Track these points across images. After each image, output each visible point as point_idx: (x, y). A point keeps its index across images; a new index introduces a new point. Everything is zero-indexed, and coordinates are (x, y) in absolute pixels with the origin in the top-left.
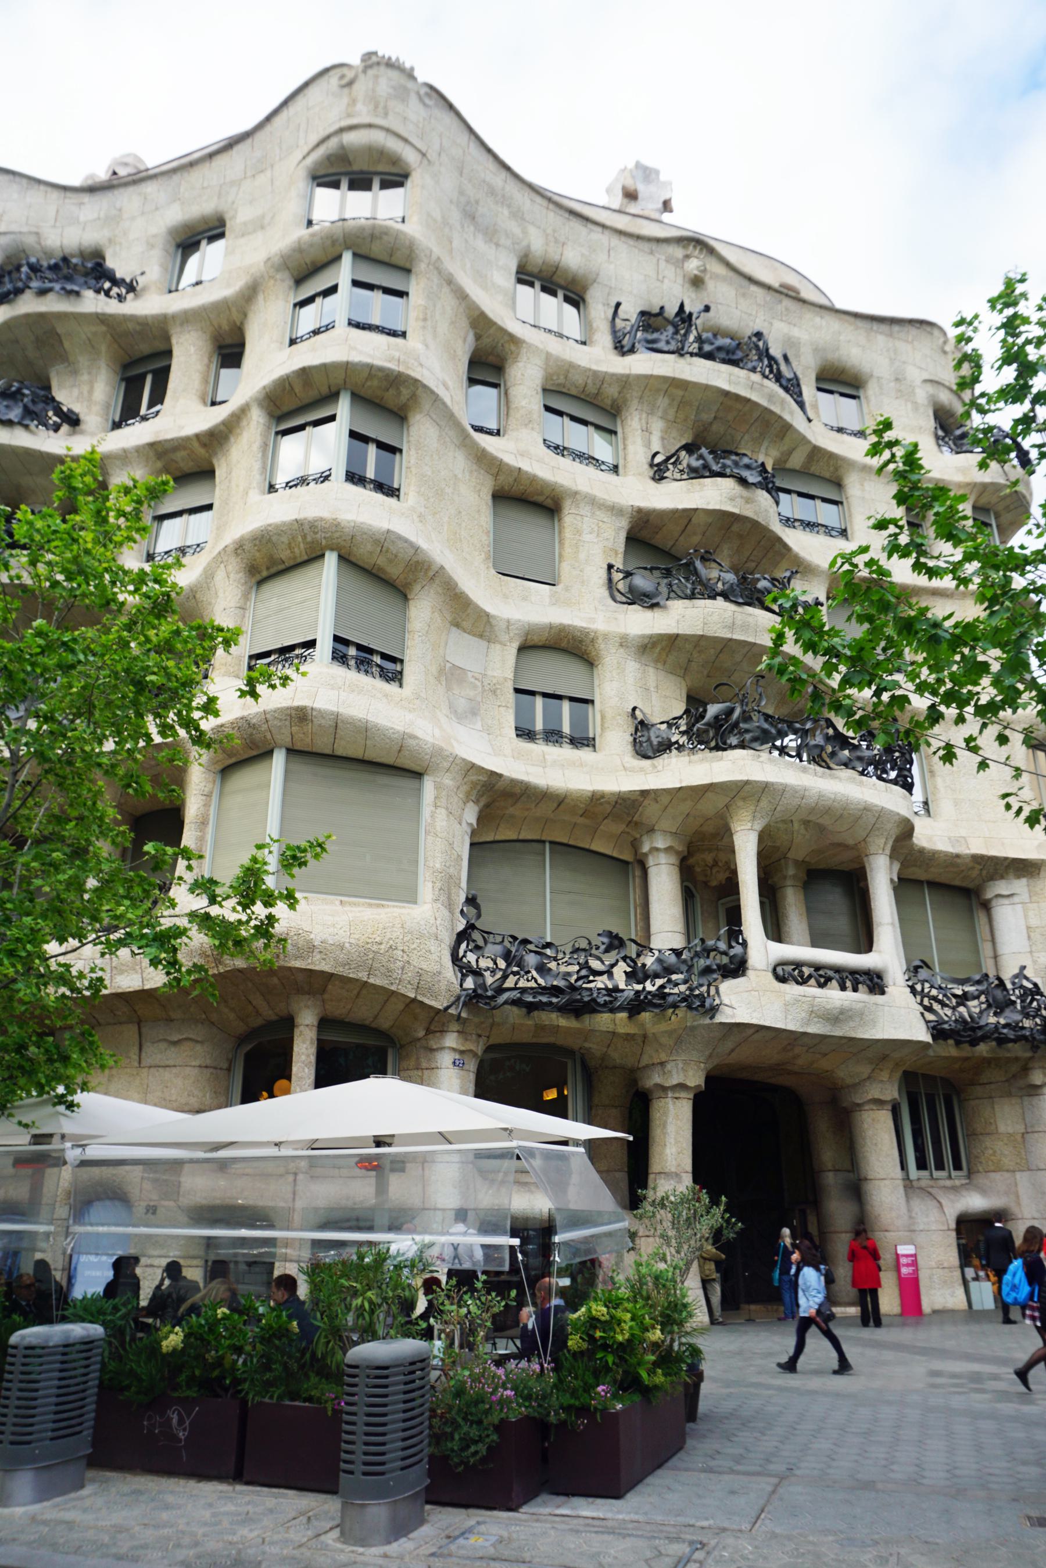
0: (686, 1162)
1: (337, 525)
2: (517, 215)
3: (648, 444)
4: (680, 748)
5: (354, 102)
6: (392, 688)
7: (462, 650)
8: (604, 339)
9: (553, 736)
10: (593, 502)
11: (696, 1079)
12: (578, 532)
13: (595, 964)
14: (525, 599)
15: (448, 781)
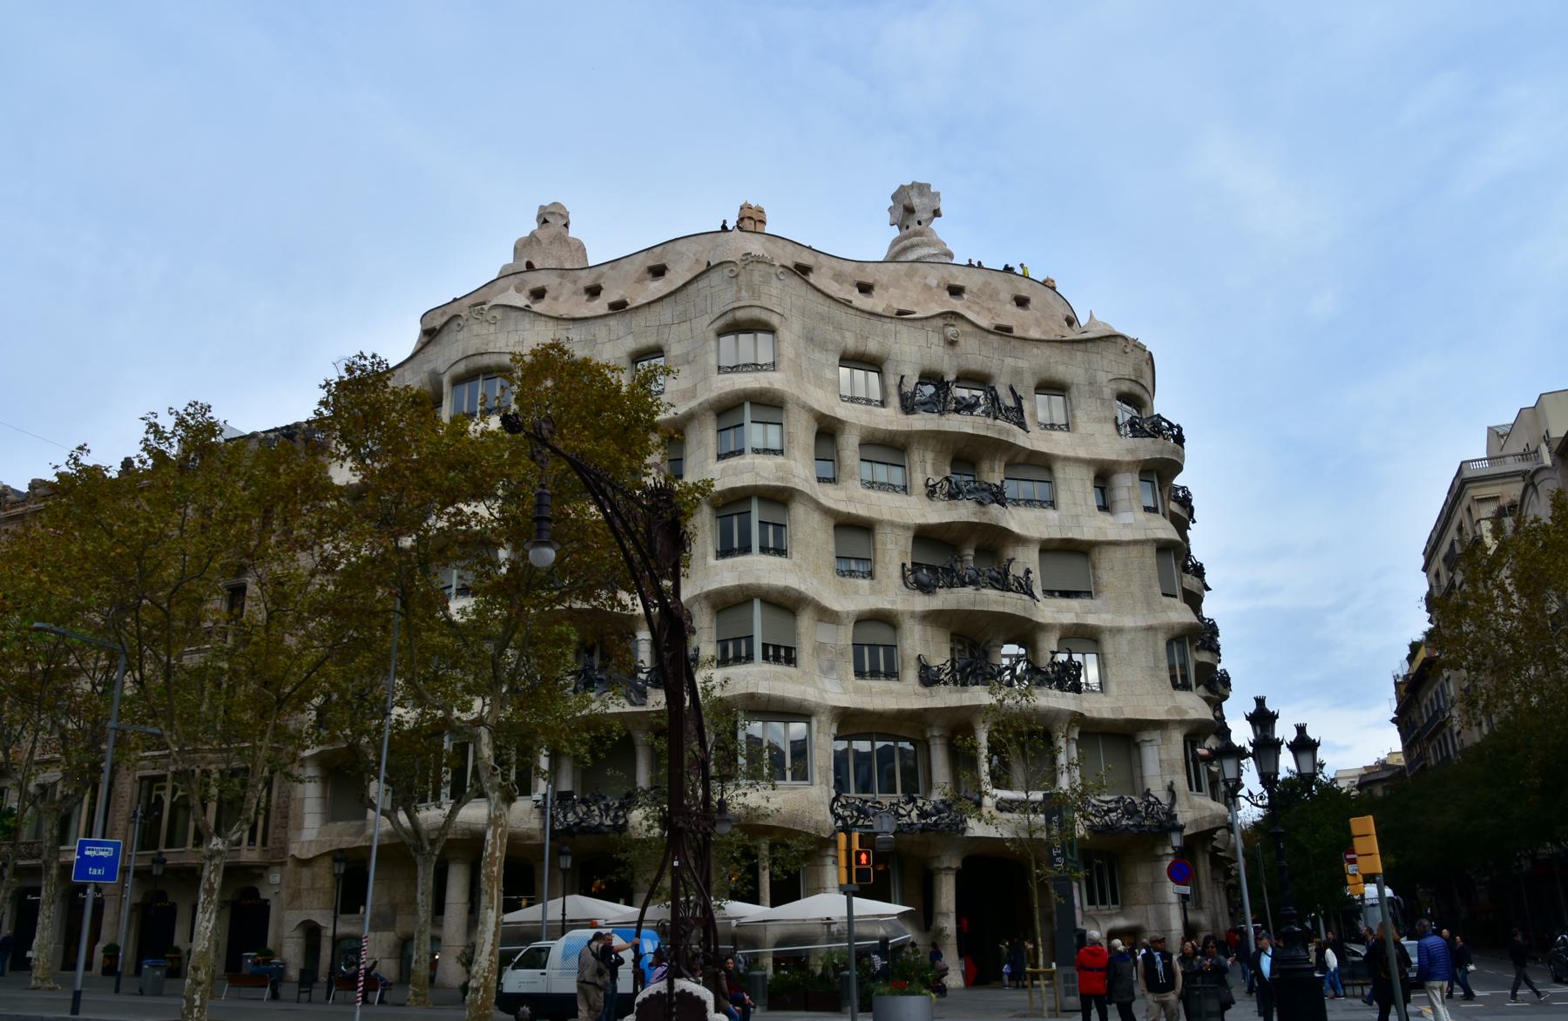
0: (952, 907)
1: (759, 587)
2: (839, 327)
3: (924, 472)
4: (945, 683)
5: (739, 290)
6: (790, 670)
7: (825, 634)
8: (894, 400)
9: (875, 674)
10: (893, 524)
11: (956, 863)
12: (884, 544)
13: (902, 812)
14: (856, 593)
15: (823, 718)
